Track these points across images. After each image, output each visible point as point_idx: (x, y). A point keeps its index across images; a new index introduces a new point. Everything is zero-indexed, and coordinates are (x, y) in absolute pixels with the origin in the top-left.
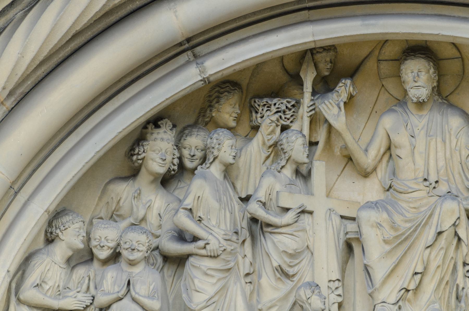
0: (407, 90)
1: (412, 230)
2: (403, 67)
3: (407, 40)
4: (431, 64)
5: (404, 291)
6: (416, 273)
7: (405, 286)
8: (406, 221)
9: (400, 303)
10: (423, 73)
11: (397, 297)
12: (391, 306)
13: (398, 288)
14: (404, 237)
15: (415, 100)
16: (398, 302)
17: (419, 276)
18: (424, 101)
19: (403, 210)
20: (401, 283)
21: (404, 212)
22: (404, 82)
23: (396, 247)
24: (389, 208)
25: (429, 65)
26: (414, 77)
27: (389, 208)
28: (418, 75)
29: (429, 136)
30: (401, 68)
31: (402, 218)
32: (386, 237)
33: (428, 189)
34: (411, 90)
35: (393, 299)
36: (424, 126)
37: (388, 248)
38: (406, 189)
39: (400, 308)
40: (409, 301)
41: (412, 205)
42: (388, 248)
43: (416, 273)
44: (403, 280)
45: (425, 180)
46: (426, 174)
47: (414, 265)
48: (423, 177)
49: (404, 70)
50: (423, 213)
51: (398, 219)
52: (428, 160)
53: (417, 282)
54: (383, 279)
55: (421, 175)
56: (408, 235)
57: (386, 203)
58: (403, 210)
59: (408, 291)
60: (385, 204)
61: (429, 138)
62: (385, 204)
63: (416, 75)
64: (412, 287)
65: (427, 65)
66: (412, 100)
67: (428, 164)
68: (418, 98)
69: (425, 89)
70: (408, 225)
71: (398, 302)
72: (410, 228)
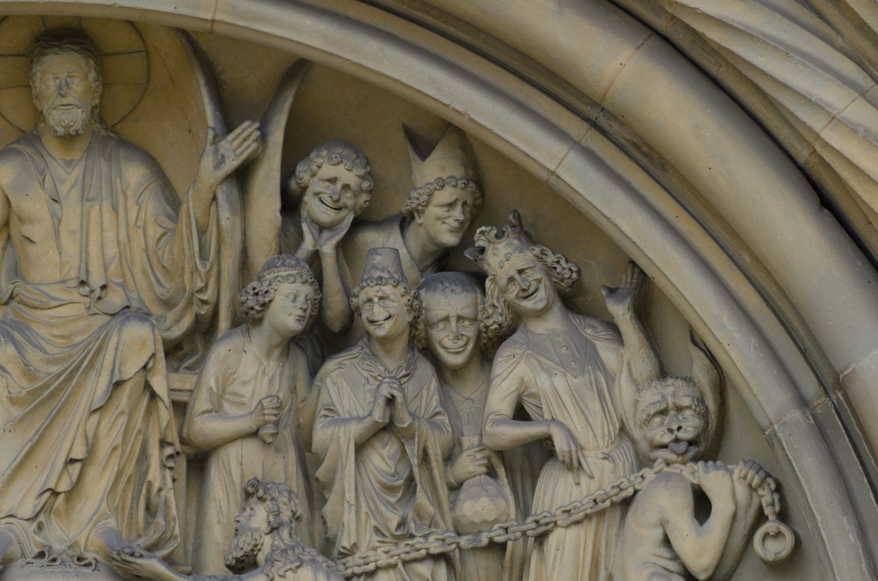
0: (45, 111)
1: (62, 378)
2: (38, 69)
3: (43, 18)
4: (92, 62)
5: (47, 494)
6: (72, 461)
7: (51, 485)
8: (49, 362)
9: (42, 518)
10: (77, 80)
11: (35, 506)
12: (25, 523)
13: (37, 489)
14: (46, 393)
15: (61, 131)
16: (37, 515)
17: (78, 466)
18: (77, 134)
19: (40, 341)
20: (43, 479)
21: (43, 344)
22: (37, 97)
23: (32, 410)
24: (17, 336)
25: (87, 65)
26: (60, 88)
27: (17, 336)
28: (67, 84)
29: (89, 200)
30: (34, 70)
31: (40, 355)
32: (12, 391)
33: (88, 300)
34: (54, 113)
35: (28, 510)
36: (76, 181)
37: (17, 412)
38: (45, 300)
39: (40, 527)
40: (58, 514)
41: (57, 332)
42: (17, 412)
43: (72, 461)
44: (46, 474)
45: (83, 283)
46: (83, 272)
47: (67, 445)
48: (78, 278)
49: (38, 74)
50: (80, 346)
51: (34, 357)
52: (87, 245)
53: (74, 478)
54: (9, 472)
55: (73, 273)
56: (56, 388)
57: (11, 327)
58: (40, 341)
59: (55, 494)
60: (10, 330)
61: (87, 204)
62: (10, 330)
63: (63, 83)
64: (64, 486)
65: (83, 63)
66: (55, 131)
67: (87, 253)
68: (68, 127)
69: (80, 111)
70: (54, 369)
71: (37, 515)
72: (59, 376)
